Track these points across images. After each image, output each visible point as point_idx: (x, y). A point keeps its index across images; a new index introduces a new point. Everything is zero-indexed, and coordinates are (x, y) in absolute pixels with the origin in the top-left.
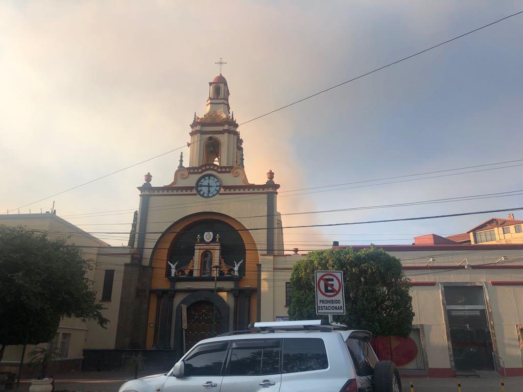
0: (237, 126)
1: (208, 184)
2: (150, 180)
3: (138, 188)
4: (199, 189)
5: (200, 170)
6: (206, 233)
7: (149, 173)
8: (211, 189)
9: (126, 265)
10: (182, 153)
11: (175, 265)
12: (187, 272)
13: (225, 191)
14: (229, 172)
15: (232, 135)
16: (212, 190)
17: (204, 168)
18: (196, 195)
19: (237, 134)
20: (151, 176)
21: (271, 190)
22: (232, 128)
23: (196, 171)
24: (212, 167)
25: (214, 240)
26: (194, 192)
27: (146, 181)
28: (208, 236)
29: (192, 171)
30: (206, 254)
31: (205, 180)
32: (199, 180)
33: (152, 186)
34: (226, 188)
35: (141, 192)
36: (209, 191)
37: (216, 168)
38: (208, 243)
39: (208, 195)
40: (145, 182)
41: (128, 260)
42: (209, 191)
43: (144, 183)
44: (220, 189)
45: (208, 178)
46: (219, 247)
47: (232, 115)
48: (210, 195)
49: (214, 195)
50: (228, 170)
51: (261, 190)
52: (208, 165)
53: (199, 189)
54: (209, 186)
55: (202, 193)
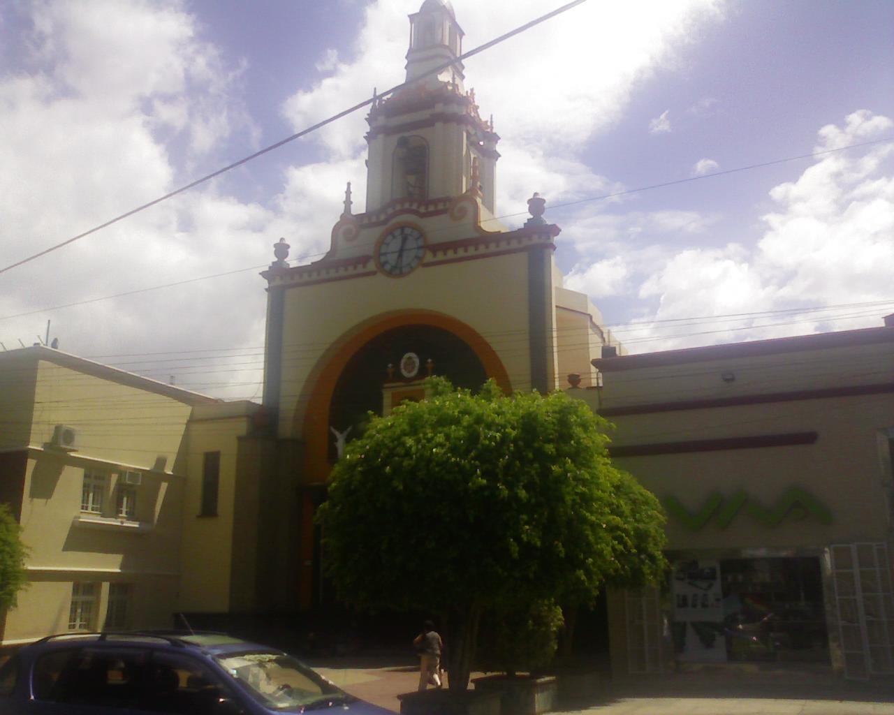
2: (287, 255)
3: (260, 274)
5: (383, 217)
7: (282, 239)
9: (240, 439)
10: (349, 184)
11: (346, 433)
13: (435, 255)
17: (390, 211)
18: (374, 273)
20: (288, 247)
21: (536, 240)
26: (371, 266)
27: (276, 253)
32: (381, 243)
33: (291, 266)
34: (435, 248)
35: (269, 283)
40: (276, 259)
41: (242, 427)
43: (273, 263)
45: (397, 233)
48: (404, 270)
49: (412, 269)
50: (441, 207)
51: (514, 244)
53: (383, 259)
55: (388, 267)
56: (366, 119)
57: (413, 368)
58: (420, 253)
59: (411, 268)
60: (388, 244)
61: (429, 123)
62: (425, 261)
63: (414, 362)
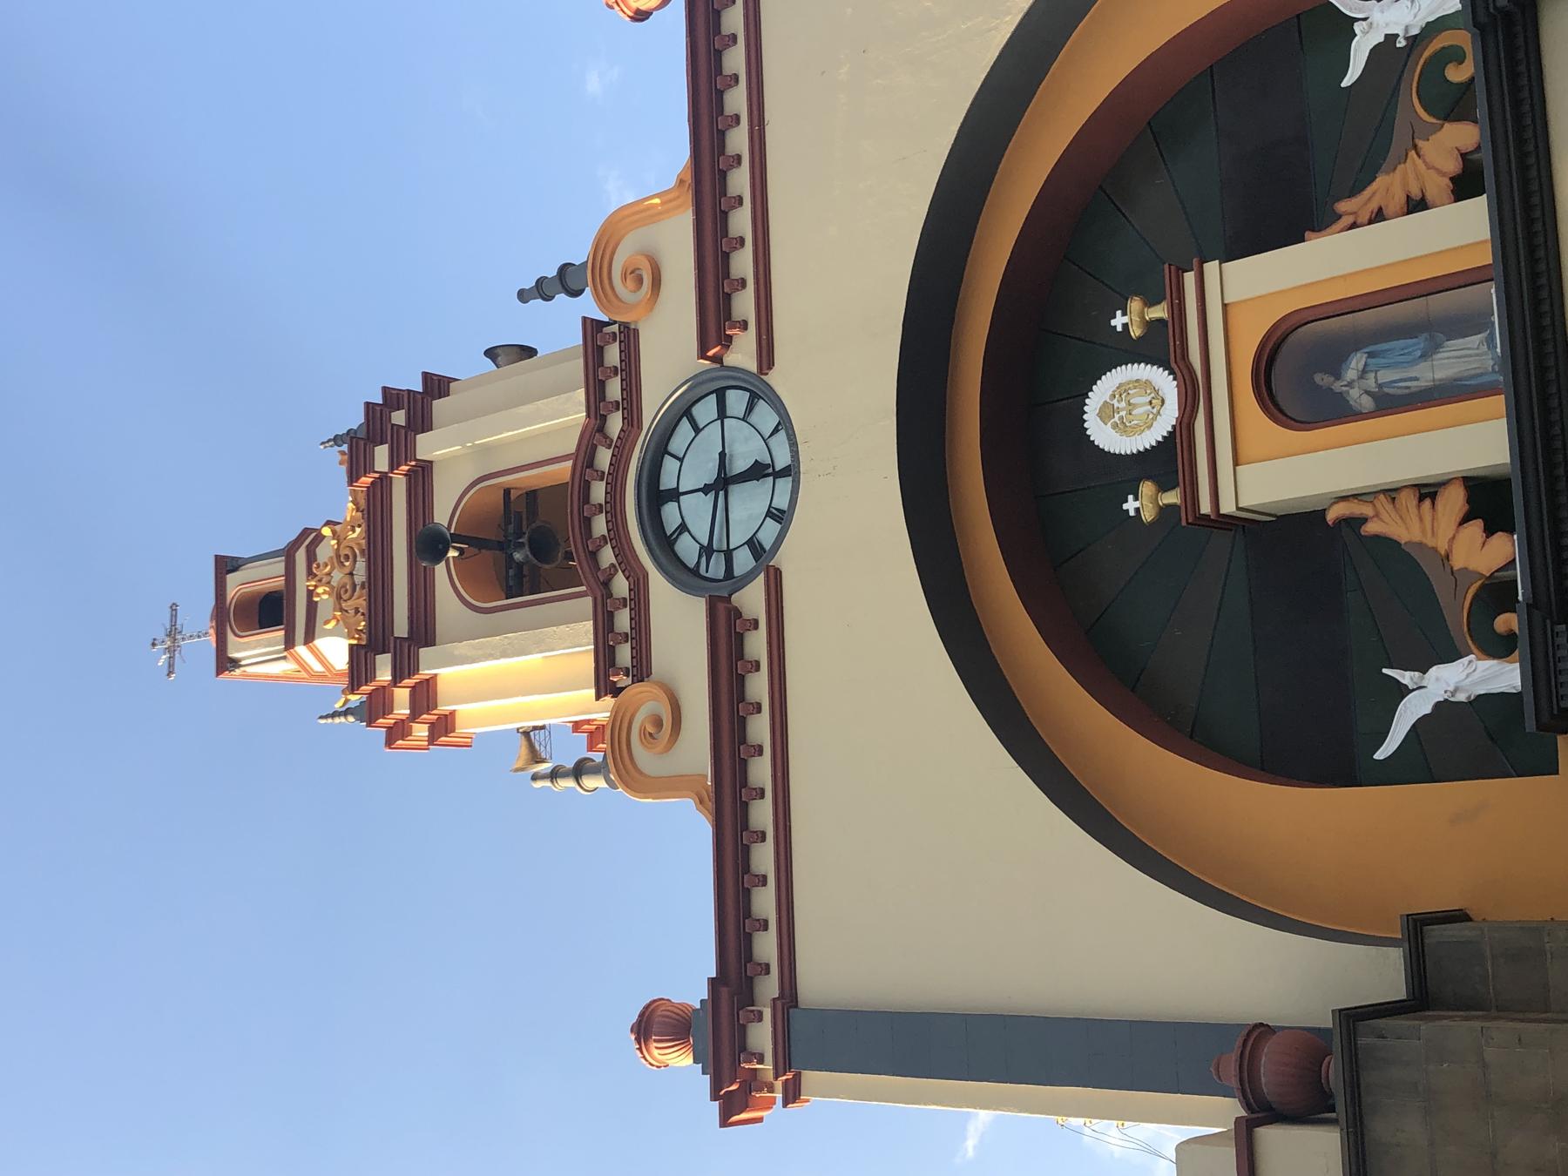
0: (392, 398)
1: (706, 489)
3: (724, 1122)
4: (743, 561)
6: (1104, 435)
8: (740, 465)
12: (1485, 553)
13: (744, 325)
14: (629, 338)
15: (438, 405)
16: (745, 452)
17: (607, 556)
19: (437, 386)
22: (399, 418)
23: (623, 620)
24: (599, 492)
25: (1162, 347)
26: (752, 599)
28: (1125, 411)
29: (624, 654)
30: (1299, 375)
31: (683, 528)
32: (685, 576)
34: (714, 325)
36: (758, 471)
37: (604, 458)
38: (1193, 394)
39: (785, 472)
42: (758, 471)
44: (739, 378)
45: (670, 513)
46: (1211, 268)
47: (337, 440)
48: (782, 459)
50: (613, 355)
52: (587, 523)
53: (743, 561)
54: (723, 483)
55: (770, 530)
56: (389, 742)
57: (1147, 385)
58: (736, 401)
59: (776, 431)
60: (702, 547)
61: (422, 476)
62: (753, 368)
63: (1122, 390)
